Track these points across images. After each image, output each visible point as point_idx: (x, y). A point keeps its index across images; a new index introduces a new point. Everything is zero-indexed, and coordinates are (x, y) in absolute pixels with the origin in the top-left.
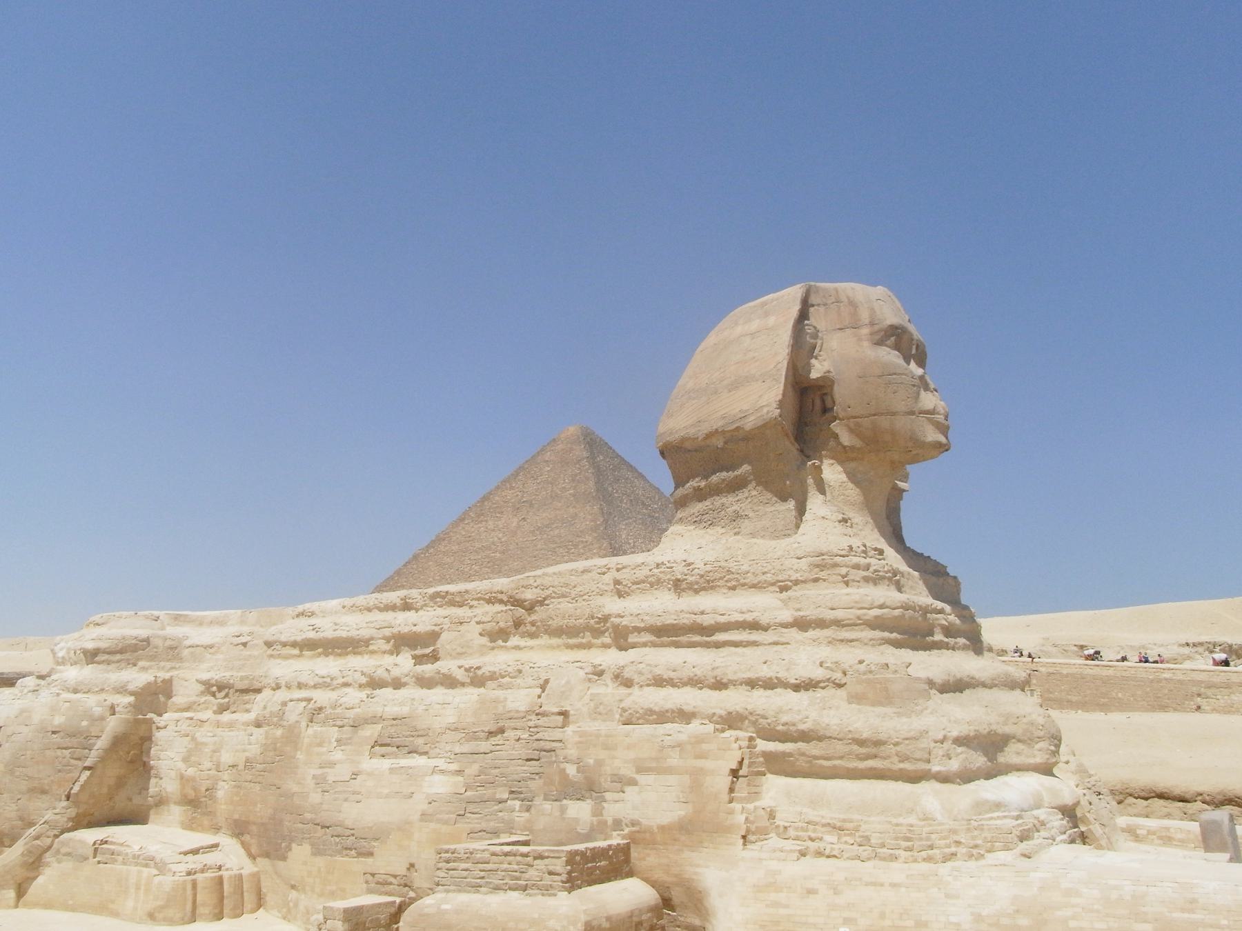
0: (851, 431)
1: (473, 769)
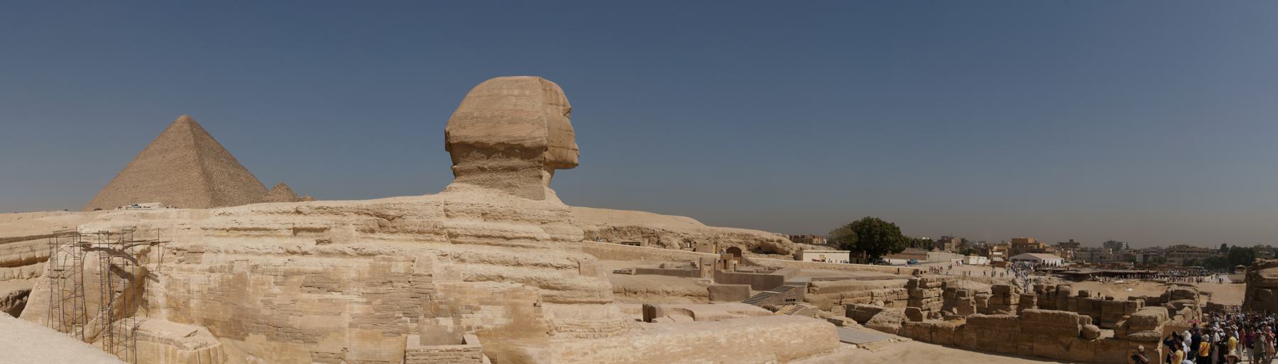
1: (379, 301)
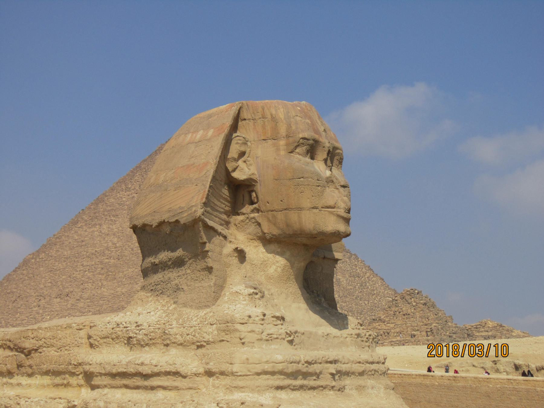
0: (269, 221)
